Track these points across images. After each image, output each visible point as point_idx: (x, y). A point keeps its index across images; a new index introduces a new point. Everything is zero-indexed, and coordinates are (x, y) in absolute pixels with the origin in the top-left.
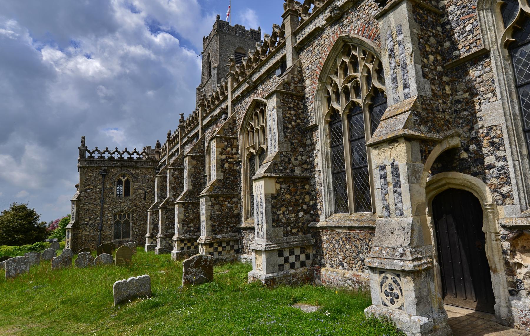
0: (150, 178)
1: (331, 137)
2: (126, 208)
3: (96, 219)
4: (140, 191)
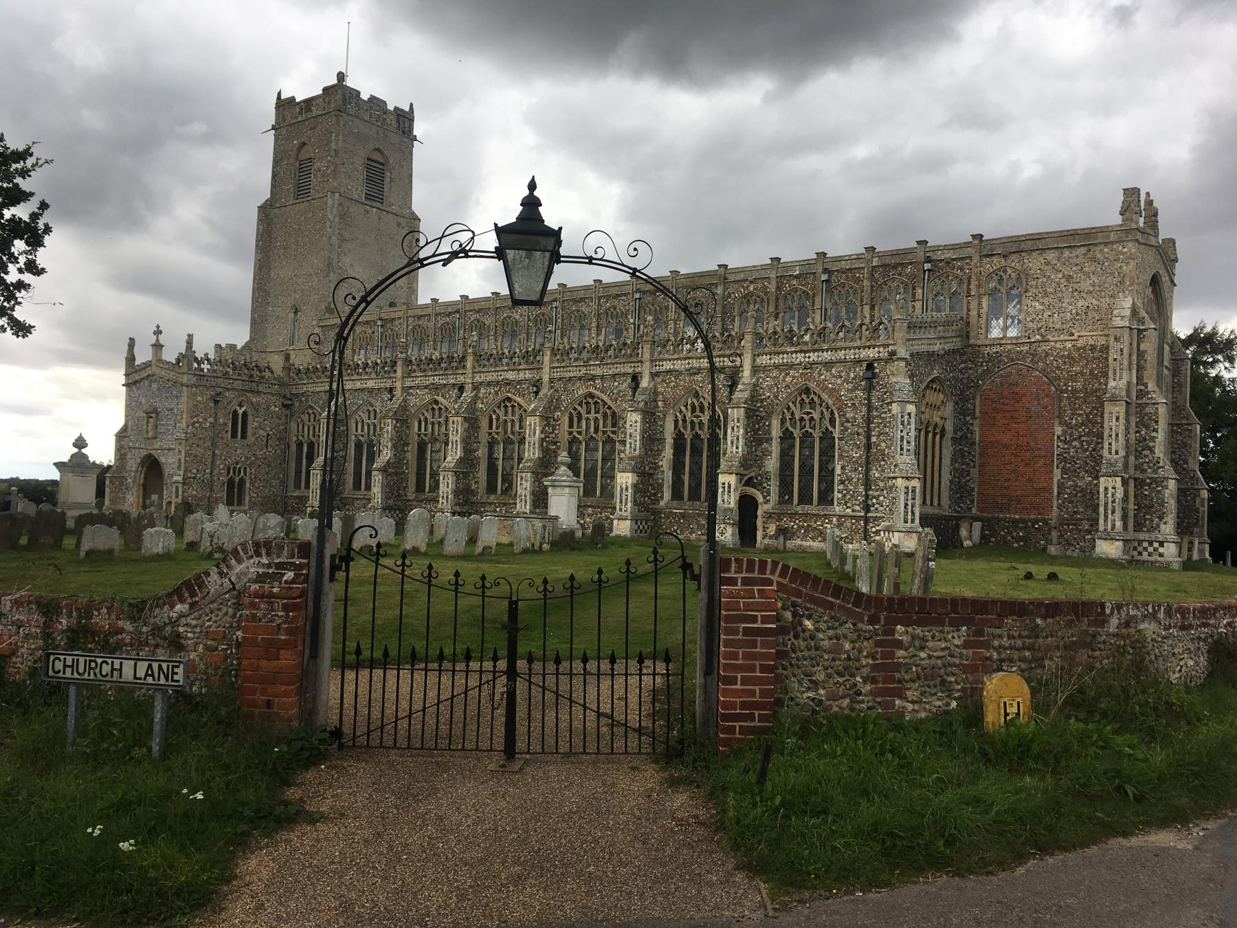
0: (275, 412)
1: (674, 449)
2: (243, 458)
3: (205, 471)
4: (261, 432)
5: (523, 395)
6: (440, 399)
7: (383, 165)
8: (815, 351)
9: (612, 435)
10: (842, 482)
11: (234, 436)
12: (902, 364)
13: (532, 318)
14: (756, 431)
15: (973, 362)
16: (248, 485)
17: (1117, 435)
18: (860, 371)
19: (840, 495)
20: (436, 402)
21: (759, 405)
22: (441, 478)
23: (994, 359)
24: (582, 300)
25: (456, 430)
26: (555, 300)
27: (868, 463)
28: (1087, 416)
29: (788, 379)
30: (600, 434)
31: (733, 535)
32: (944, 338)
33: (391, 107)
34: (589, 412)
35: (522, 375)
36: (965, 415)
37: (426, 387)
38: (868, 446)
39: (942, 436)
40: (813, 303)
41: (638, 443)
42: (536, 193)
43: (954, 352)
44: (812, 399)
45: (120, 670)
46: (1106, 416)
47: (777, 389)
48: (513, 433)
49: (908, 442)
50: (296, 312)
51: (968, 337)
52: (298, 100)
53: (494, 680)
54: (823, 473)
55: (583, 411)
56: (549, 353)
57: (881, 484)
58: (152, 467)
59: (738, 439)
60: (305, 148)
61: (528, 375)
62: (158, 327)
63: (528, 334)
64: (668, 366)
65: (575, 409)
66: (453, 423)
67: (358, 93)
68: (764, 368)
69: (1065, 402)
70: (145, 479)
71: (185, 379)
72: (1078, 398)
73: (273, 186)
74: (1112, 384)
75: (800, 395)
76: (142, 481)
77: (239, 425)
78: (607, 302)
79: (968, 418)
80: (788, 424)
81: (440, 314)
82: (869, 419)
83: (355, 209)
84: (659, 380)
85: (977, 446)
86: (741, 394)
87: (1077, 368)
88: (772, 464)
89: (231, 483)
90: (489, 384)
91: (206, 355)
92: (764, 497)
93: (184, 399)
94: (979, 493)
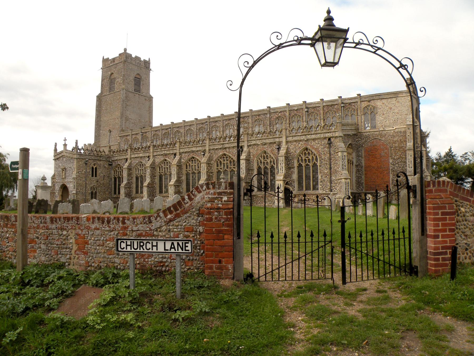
5: (199, 156)
6: (167, 159)
7: (140, 79)
8: (309, 135)
9: (233, 169)
10: (321, 182)
11: (92, 176)
12: (341, 138)
13: (198, 129)
14: (288, 165)
15: (360, 138)
16: (98, 194)
17: (411, 161)
18: (326, 141)
19: (321, 186)
20: (166, 160)
21: (289, 155)
22: (170, 188)
23: (368, 137)
24: (216, 121)
25: (174, 171)
26: (207, 122)
27: (331, 174)
28: (400, 156)
29: (300, 145)
30: (229, 168)
31: (283, 203)
32: (352, 130)
33: (142, 59)
34: (224, 161)
35: (198, 149)
36: (359, 157)
37: (162, 155)
38: (331, 168)
39: (353, 164)
40: (303, 119)
41: (244, 171)
42: (331, 15)
43: (354, 135)
44: (309, 152)
45: (157, 246)
46: (407, 155)
47: (296, 149)
48: (195, 170)
49: (345, 166)
50: (110, 132)
51: (358, 129)
52: (110, 59)
53: (325, 246)
54: (314, 179)
55: (222, 160)
56: (208, 140)
57: (336, 182)
58: (64, 188)
59: (282, 167)
60: (113, 75)
61: (200, 148)
62: (65, 138)
63: (196, 134)
64: (254, 142)
65: (219, 160)
66: (173, 167)
67: (131, 55)
68: (291, 142)
69: (393, 151)
70: (62, 193)
71: (75, 156)
72: (397, 150)
73: (102, 89)
74: (408, 144)
75: (304, 151)
76: (61, 194)
77: (94, 172)
78: (226, 122)
79: (360, 158)
80: (300, 162)
81: (163, 129)
82: (330, 158)
83: (131, 95)
84: (251, 147)
85: (364, 168)
86: (283, 151)
87: (395, 139)
88: (295, 176)
89: (92, 193)
90: (186, 152)
91: (82, 147)
92: (293, 189)
93: (75, 163)
94: (365, 184)
